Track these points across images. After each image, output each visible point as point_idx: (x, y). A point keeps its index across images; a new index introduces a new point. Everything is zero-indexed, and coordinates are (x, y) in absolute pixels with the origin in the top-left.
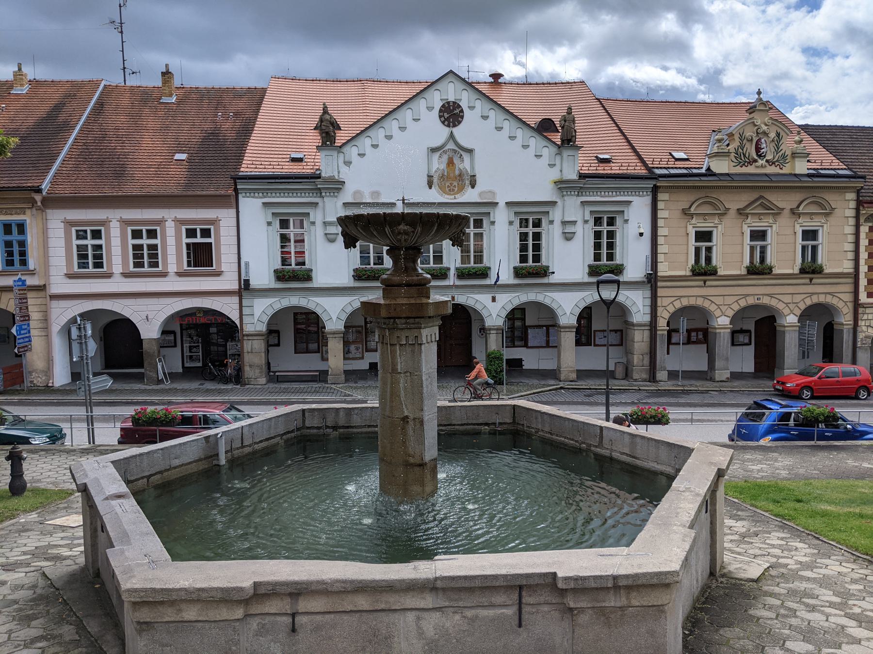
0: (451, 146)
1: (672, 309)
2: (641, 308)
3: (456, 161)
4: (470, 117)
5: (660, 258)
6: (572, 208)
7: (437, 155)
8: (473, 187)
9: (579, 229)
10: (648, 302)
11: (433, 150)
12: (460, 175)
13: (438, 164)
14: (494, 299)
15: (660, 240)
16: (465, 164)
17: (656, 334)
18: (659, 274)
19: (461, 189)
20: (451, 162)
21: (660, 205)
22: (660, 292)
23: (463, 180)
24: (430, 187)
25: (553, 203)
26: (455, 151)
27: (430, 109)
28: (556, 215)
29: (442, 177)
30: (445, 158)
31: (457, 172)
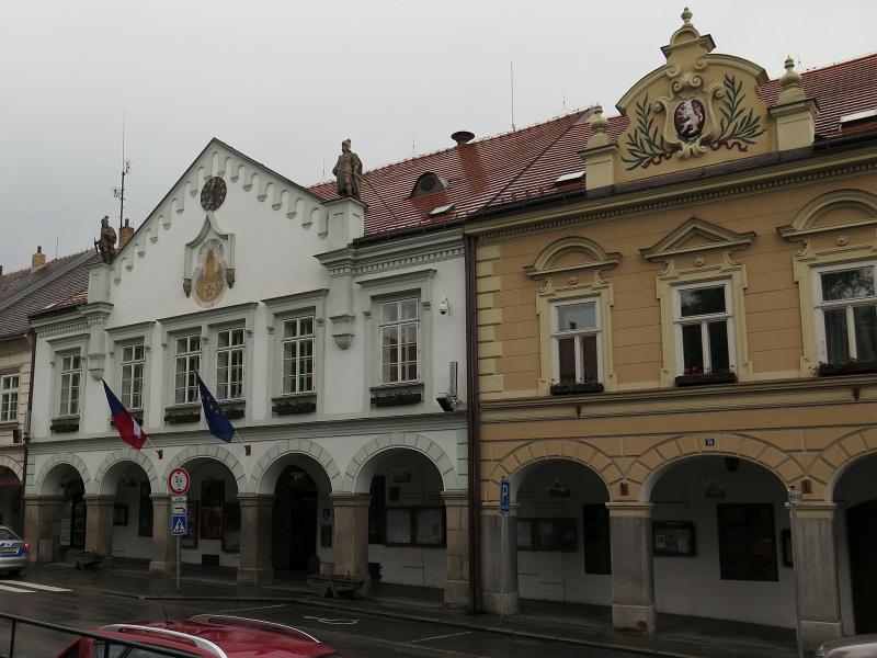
0: (210, 236)
1: (512, 465)
2: (455, 462)
3: (215, 255)
4: (233, 191)
5: (486, 366)
6: (347, 296)
7: (197, 250)
8: (231, 287)
9: (359, 329)
10: (464, 453)
11: (191, 245)
12: (219, 273)
13: (197, 262)
14: (248, 450)
15: (485, 333)
16: (223, 259)
17: (480, 517)
18: (483, 397)
19: (219, 291)
20: (210, 257)
21: (483, 269)
22: (487, 432)
23: (220, 279)
24: (188, 296)
25: (322, 293)
26: (214, 241)
27: (193, 193)
28: (336, 305)
29: (202, 279)
30: (205, 251)
31: (216, 270)
